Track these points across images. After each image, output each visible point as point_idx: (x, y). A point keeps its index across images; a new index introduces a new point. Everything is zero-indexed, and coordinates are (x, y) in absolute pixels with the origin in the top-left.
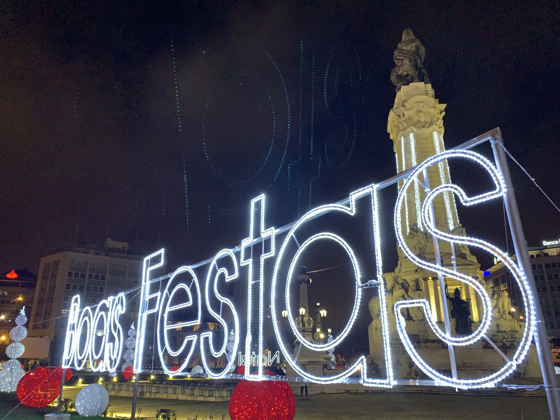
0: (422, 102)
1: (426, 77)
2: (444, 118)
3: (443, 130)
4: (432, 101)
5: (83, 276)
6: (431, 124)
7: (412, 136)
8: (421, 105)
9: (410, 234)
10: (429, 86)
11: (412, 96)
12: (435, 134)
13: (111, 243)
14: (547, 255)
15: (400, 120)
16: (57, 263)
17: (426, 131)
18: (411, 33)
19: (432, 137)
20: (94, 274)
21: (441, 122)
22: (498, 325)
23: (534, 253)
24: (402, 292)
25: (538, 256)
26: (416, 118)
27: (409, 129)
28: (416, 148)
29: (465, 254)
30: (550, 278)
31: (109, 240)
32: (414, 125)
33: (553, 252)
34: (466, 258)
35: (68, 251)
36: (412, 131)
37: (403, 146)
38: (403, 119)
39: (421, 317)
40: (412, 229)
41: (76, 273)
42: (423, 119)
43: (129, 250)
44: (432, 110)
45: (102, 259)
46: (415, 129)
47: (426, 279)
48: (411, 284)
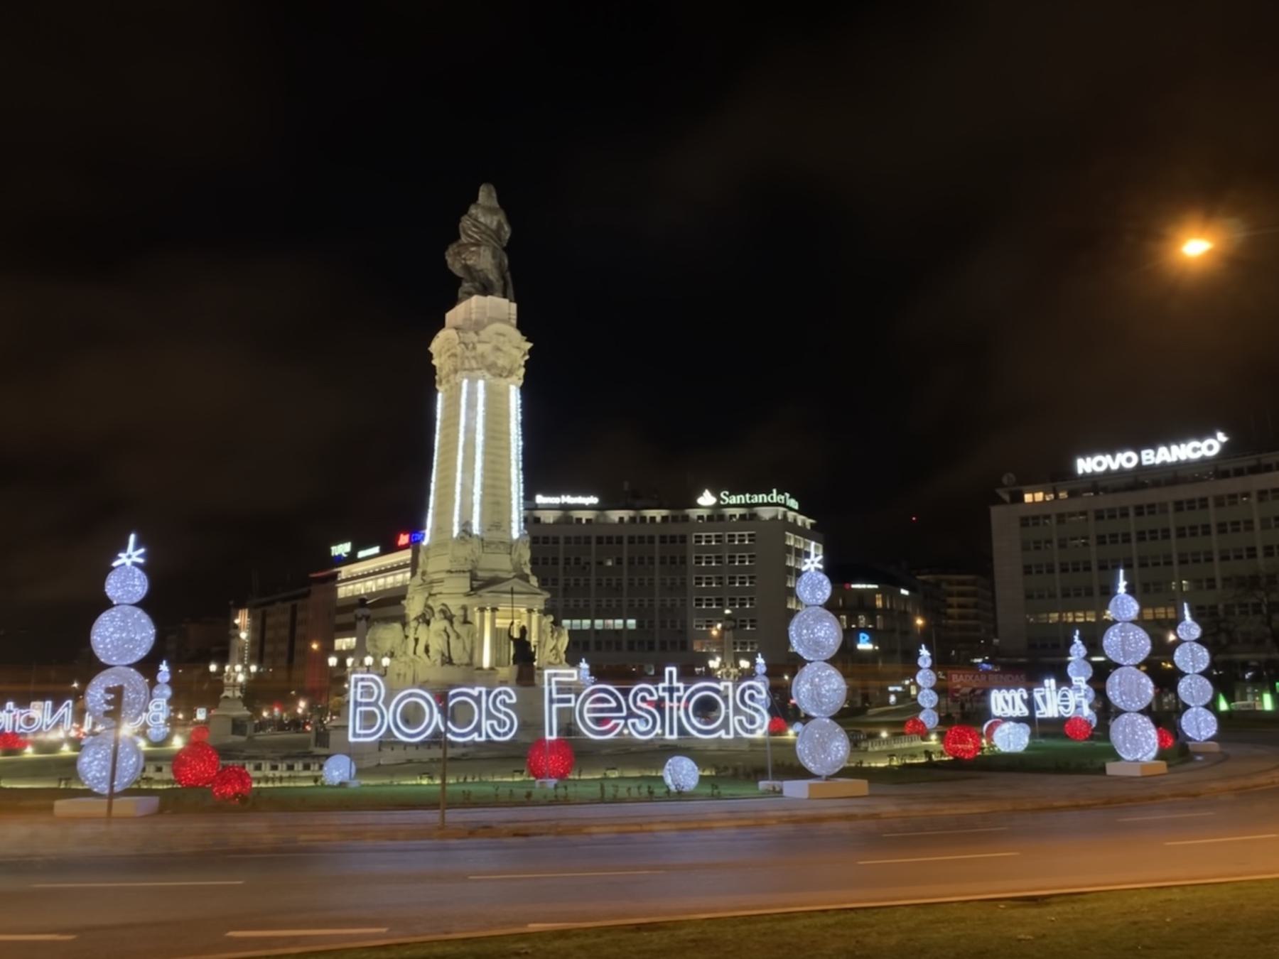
0: (503, 335)
1: (510, 291)
2: (527, 365)
3: (521, 382)
4: (516, 335)
6: (511, 373)
7: (481, 384)
8: (502, 339)
9: (462, 538)
10: (514, 306)
11: (493, 320)
15: (468, 354)
17: (503, 382)
19: (508, 391)
21: (522, 371)
24: (446, 623)
26: (491, 359)
27: (479, 373)
36: (483, 378)
38: (473, 354)
39: (466, 660)
40: (464, 531)
42: (501, 362)
46: (488, 376)
47: (482, 610)
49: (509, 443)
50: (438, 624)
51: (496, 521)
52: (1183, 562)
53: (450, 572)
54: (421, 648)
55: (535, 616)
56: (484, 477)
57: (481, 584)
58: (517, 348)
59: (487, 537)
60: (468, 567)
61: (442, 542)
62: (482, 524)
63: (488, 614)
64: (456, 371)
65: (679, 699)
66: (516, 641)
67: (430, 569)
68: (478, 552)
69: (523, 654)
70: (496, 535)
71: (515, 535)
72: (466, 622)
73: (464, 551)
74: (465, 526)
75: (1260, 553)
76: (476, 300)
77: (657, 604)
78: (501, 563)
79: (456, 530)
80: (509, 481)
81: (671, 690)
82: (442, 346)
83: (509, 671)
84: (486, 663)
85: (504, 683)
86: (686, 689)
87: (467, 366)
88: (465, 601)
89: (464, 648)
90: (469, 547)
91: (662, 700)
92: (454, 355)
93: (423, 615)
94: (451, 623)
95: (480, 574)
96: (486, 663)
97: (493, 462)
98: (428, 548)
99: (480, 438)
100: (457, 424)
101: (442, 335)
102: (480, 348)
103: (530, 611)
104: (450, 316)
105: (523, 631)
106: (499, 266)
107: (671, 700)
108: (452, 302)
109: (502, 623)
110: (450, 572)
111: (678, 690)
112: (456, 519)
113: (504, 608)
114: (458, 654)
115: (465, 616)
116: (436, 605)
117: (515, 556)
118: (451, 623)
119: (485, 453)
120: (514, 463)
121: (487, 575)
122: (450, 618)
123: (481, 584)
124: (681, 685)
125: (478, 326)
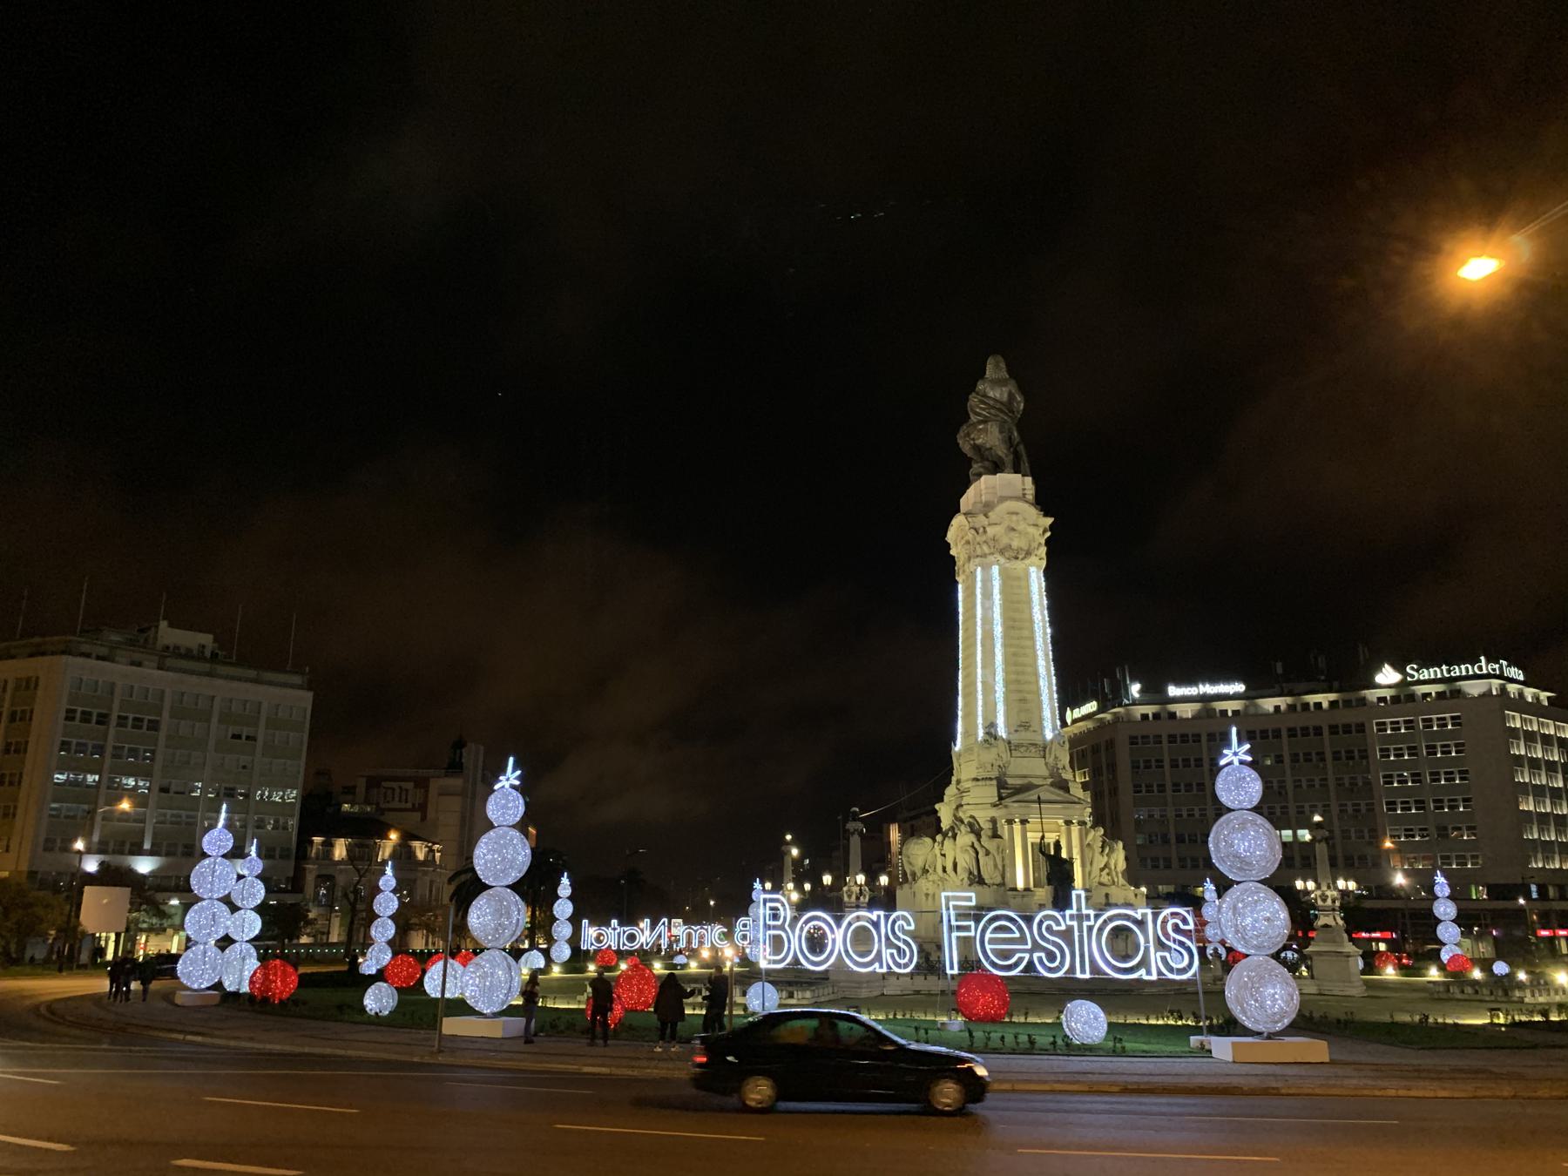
1: (1025, 465)
2: (1048, 542)
3: (1044, 563)
4: (1033, 513)
5: (103, 719)
6: (1028, 554)
7: (995, 570)
8: (1014, 518)
10: (1029, 480)
11: (1003, 499)
12: (1033, 569)
13: (168, 634)
14: (1173, 715)
15: (978, 539)
16: (28, 685)
17: (1018, 565)
18: (1003, 365)
19: (1027, 575)
20: (131, 716)
21: (1043, 550)
22: (1107, 895)
23: (1149, 710)
24: (972, 838)
25: (1156, 716)
26: (1005, 541)
27: (991, 558)
28: (1002, 592)
29: (1066, 781)
30: (1174, 765)
31: (163, 624)
32: (1002, 552)
33: (1186, 711)
34: (1067, 790)
35: (63, 653)
37: (979, 584)
39: (999, 880)
41: (83, 713)
42: (1015, 544)
43: (214, 655)
44: (1032, 530)
45: (151, 677)
46: (1002, 560)
47: (1010, 822)
48: (986, 826)
49: (1032, 631)
50: (965, 838)
51: (1025, 720)
53: (976, 780)
55: (1075, 829)
56: (1006, 671)
58: (1035, 527)
59: (1015, 739)
60: (995, 773)
61: (968, 749)
62: (1007, 725)
63: (1017, 827)
64: (969, 559)
65: (1090, 928)
66: (1048, 857)
67: (963, 777)
68: (1005, 756)
69: (1057, 873)
70: (1025, 736)
71: (1049, 735)
72: (995, 835)
73: (990, 756)
74: (990, 727)
76: (985, 480)
77: (1171, 813)
78: (1035, 768)
79: (981, 734)
80: (1036, 674)
81: (1080, 918)
82: (957, 530)
83: (1044, 893)
85: (1042, 907)
86: (1097, 917)
87: (979, 552)
88: (994, 813)
89: (996, 866)
90: (994, 751)
91: (1070, 929)
92: (968, 542)
93: (952, 828)
94: (979, 837)
95: (1010, 781)
96: (1020, 885)
97: (1014, 655)
98: (960, 755)
99: (998, 630)
100: (974, 616)
103: (1068, 823)
104: (962, 501)
105: (1058, 845)
106: (1009, 441)
107: (1081, 930)
109: (1033, 837)
110: (976, 780)
111: (1088, 917)
112: (980, 720)
113: (1034, 820)
115: (995, 829)
117: (1050, 760)
118: (979, 837)
119: (1005, 645)
120: (1040, 653)
121: (1019, 782)
122: (976, 831)
123: (1008, 790)
124: (1092, 913)
125: (987, 508)
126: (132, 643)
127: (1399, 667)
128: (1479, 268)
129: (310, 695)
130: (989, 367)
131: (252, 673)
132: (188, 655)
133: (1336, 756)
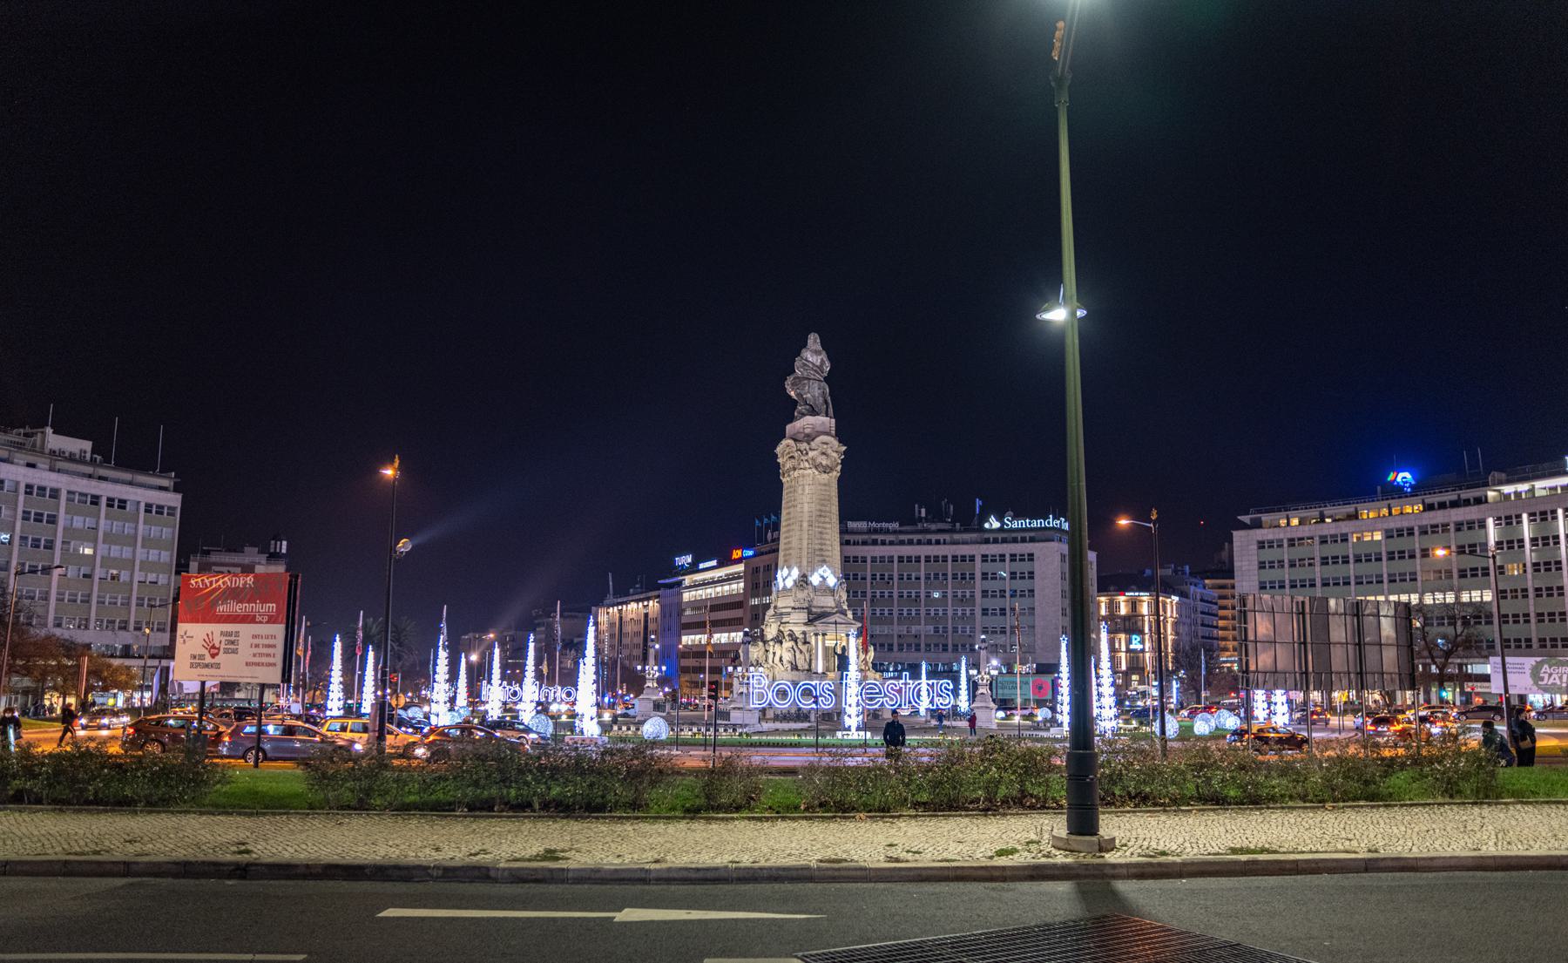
1: (831, 411)
4: (835, 442)
24: (791, 644)
50: (788, 644)
52: (1392, 581)
54: (777, 659)
57: (815, 617)
67: (780, 604)
72: (805, 643)
75: (1455, 575)
76: (809, 419)
78: (828, 602)
82: (784, 447)
84: (820, 670)
88: (804, 628)
96: (820, 670)
101: (784, 442)
102: (811, 454)
105: (844, 649)
108: (792, 419)
114: (801, 663)
116: (786, 630)
123: (815, 617)
126: (20, 447)
127: (1000, 519)
128: (1123, 522)
129: (179, 497)
130: (810, 342)
131: (127, 476)
132: (71, 458)
133: (955, 577)
